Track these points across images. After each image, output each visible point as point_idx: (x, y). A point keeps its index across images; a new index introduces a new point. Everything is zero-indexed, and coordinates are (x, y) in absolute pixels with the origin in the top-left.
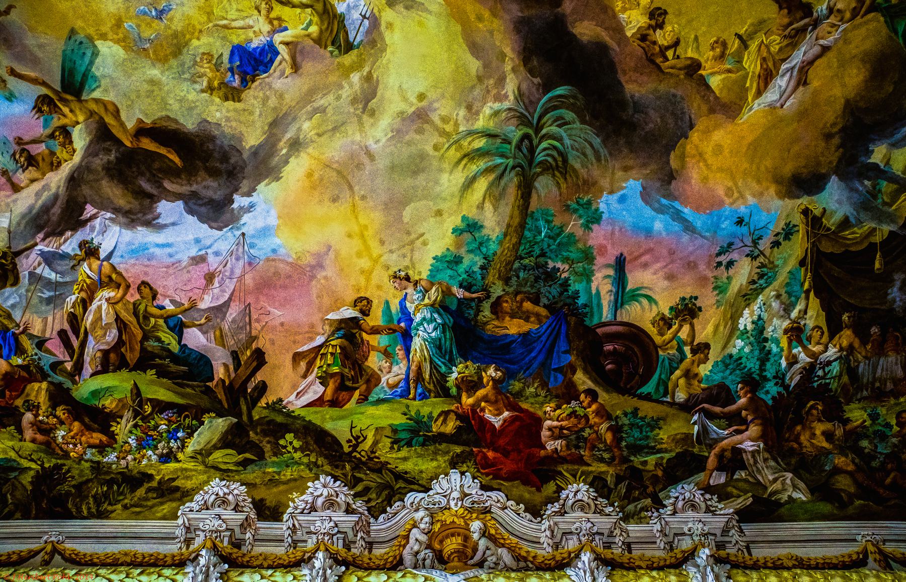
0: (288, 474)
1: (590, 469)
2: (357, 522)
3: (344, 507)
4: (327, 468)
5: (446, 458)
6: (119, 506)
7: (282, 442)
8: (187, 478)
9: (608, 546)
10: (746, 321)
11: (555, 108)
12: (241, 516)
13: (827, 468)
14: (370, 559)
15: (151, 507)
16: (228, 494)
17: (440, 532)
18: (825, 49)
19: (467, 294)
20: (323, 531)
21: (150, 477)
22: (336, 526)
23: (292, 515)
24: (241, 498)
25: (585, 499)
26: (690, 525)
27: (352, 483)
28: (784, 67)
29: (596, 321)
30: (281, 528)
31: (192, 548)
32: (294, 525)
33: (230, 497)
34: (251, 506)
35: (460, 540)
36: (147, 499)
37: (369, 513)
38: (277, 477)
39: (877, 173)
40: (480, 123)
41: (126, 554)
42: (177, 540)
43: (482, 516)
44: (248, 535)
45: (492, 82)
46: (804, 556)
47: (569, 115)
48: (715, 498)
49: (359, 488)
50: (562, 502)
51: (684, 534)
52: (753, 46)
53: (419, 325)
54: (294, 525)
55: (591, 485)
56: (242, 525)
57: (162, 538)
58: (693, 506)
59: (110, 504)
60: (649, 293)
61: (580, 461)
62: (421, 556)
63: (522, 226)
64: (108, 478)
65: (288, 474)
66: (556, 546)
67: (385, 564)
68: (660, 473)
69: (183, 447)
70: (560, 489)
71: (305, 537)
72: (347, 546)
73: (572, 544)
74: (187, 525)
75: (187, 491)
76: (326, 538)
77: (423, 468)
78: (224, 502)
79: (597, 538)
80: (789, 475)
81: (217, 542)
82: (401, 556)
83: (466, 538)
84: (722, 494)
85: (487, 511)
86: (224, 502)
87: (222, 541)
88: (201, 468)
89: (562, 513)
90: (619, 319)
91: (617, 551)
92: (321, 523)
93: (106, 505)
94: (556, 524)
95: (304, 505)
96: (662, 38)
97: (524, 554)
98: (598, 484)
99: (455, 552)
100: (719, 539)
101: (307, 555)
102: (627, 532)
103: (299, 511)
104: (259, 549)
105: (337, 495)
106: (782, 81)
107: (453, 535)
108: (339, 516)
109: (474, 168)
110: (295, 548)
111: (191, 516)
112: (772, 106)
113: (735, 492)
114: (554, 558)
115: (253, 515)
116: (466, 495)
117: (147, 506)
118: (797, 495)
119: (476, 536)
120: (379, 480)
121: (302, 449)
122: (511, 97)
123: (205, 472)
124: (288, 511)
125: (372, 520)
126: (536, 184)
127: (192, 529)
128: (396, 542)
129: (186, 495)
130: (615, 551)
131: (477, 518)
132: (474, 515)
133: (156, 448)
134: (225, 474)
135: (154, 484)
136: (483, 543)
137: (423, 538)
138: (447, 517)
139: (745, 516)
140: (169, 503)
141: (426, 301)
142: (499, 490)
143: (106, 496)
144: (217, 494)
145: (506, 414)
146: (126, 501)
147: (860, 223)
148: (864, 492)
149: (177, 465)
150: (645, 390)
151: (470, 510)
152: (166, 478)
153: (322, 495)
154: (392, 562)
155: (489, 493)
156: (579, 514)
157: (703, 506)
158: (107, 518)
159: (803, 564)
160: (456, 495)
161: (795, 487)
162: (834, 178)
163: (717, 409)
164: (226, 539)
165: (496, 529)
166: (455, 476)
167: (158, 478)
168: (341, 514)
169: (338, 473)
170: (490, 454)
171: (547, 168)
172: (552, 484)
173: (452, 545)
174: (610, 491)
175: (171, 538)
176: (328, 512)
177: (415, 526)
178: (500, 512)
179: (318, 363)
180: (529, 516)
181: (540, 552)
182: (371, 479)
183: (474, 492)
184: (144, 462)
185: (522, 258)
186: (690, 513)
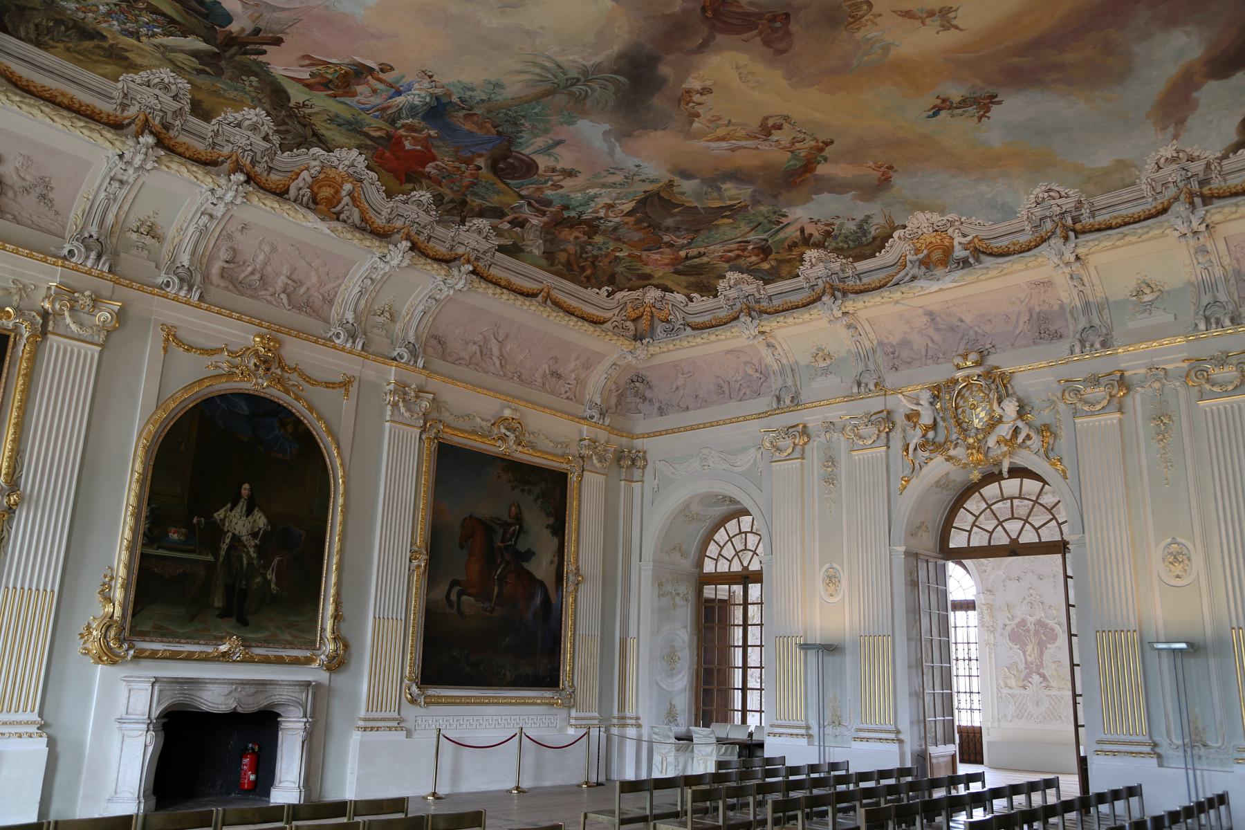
0: (233, 94)
1: (440, 188)
2: (268, 149)
3: (263, 134)
4: (267, 106)
5: (358, 142)
6: (61, 45)
7: (244, 78)
8: (140, 55)
9: (418, 233)
10: (592, 192)
11: (608, 81)
12: (178, 106)
13: (561, 247)
14: (267, 180)
15: (95, 62)
16: (173, 84)
17: (322, 180)
18: (757, 148)
19: (459, 103)
20: (239, 144)
21: (104, 38)
22: (251, 145)
23: (219, 123)
24: (182, 92)
25: (424, 202)
26: (470, 241)
27: (278, 122)
28: (734, 142)
29: (518, 150)
30: (208, 129)
31: (126, 114)
32: (218, 130)
33: (173, 87)
34: (189, 101)
35: (332, 191)
36: (93, 53)
37: (280, 147)
38: (222, 92)
39: (719, 189)
40: (561, 59)
41: (63, 94)
42: (114, 101)
43: (355, 182)
44: (178, 122)
45: (590, 51)
46: (513, 282)
47: (611, 87)
48: (494, 233)
49: (282, 128)
50: (409, 196)
51: (463, 244)
52: (731, 128)
53: (412, 94)
54: (218, 130)
55: (434, 196)
56: (174, 112)
57: (100, 93)
58: (480, 232)
59: (52, 39)
60: (559, 157)
61: (440, 184)
62: (302, 192)
63: (527, 102)
64: (58, 17)
65: (233, 94)
66: (389, 221)
67: (276, 189)
68: (477, 209)
69: (154, 35)
70: (414, 189)
71: (224, 143)
72: (254, 162)
73: (399, 223)
74: (125, 91)
75: (136, 65)
76: (240, 151)
77: (337, 138)
78: (166, 88)
79: (416, 225)
80: (541, 241)
81: (150, 119)
82: (289, 186)
83: (337, 192)
84: (499, 234)
85: (361, 181)
86: (166, 88)
87: (154, 119)
88: (159, 55)
89: (405, 202)
90: (531, 156)
91: (422, 238)
92: (241, 138)
93: (47, 38)
94: (397, 207)
95: (233, 120)
96: (696, 98)
97: (368, 218)
98: (438, 200)
99: (326, 198)
100: (480, 255)
101: (220, 159)
102: (434, 230)
103: (226, 122)
104: (183, 138)
105: (263, 125)
106: (724, 144)
107: (330, 186)
108: (257, 140)
109: (532, 69)
110: (213, 149)
111: (132, 85)
112: (708, 147)
113: (507, 235)
114: (383, 228)
115: (187, 108)
116: (353, 166)
117: (90, 58)
118: (534, 251)
119: (344, 193)
120: (300, 130)
121: (256, 88)
122: (591, 63)
123: (160, 59)
124: (218, 118)
125: (279, 152)
126: (557, 95)
127: (129, 97)
128: (289, 175)
129: (134, 67)
130: (420, 238)
131: (351, 182)
132: (351, 180)
133: (125, 24)
134: (178, 69)
135: (105, 45)
136: (346, 199)
137: (309, 180)
138: (332, 173)
139: (502, 249)
140: (113, 66)
141: (430, 90)
142: (377, 173)
143: (49, 30)
144: (162, 80)
145: (419, 148)
146: (70, 45)
147: (689, 196)
148: (569, 265)
149: (136, 43)
150: (509, 181)
151: (350, 175)
152: (119, 46)
153: (251, 119)
154: (281, 188)
155: (368, 172)
156: (415, 208)
157: (485, 234)
158: (46, 49)
159: (510, 288)
160: (347, 163)
161: (538, 247)
162: (699, 181)
163: (537, 205)
164: (158, 119)
165: (359, 194)
166: (355, 152)
167: (111, 42)
168: (259, 138)
169: (273, 112)
170: (388, 154)
171: (572, 95)
172: (412, 185)
173: (326, 192)
174: (442, 204)
175: (109, 97)
176: (249, 133)
177: (307, 169)
178: (368, 185)
179: (320, 67)
180: (384, 195)
181: (378, 221)
182: (294, 126)
183: (360, 167)
184: (104, 25)
185: (510, 110)
186: (475, 235)
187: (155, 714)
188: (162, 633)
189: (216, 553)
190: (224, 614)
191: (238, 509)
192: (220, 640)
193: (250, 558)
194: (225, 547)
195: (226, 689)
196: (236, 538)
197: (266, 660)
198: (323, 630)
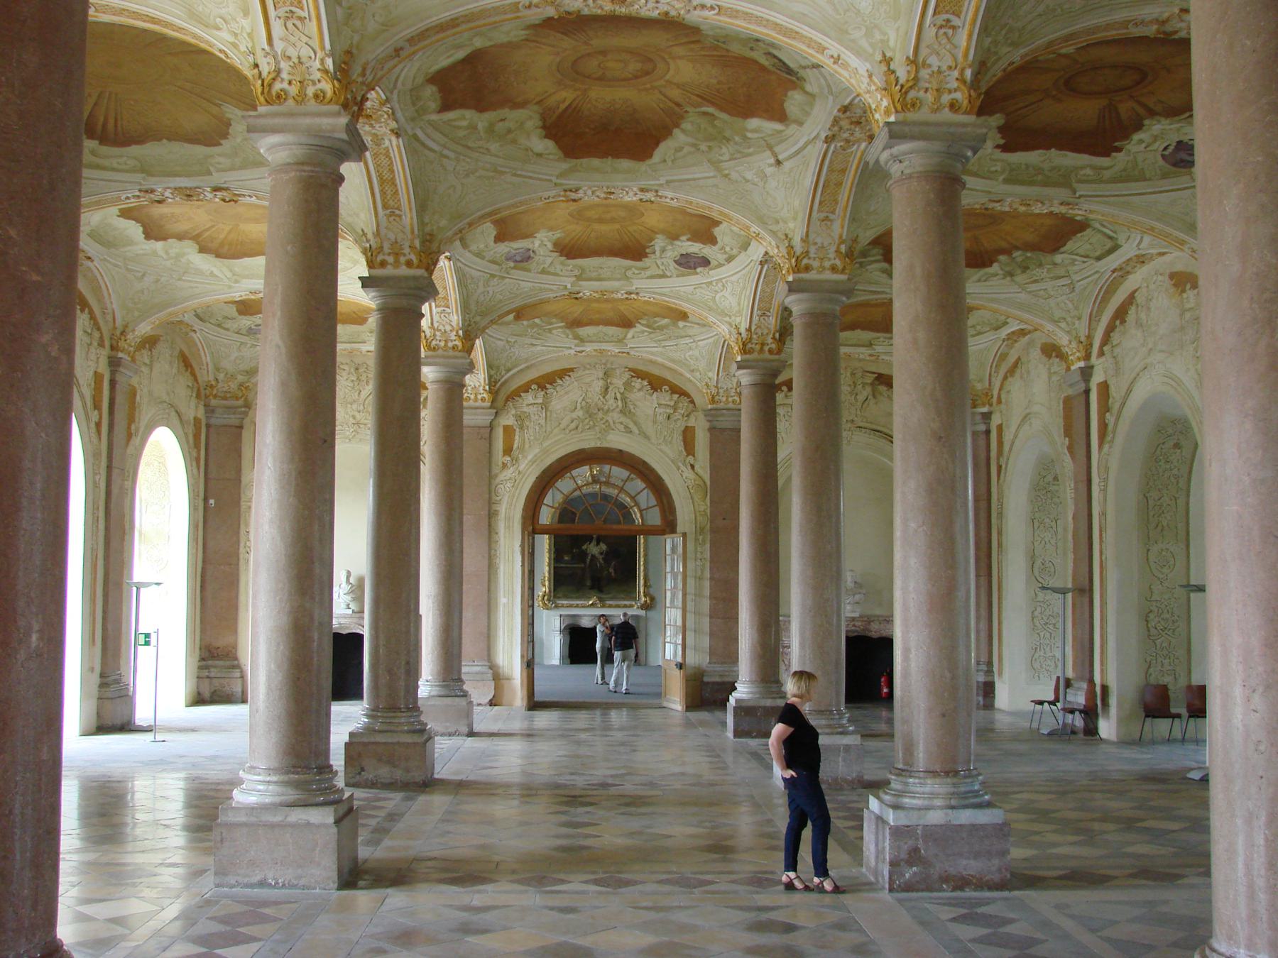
187: (562, 628)
188: (566, 597)
189: (585, 562)
190: (592, 588)
191: (592, 544)
192: (590, 598)
193: (601, 564)
194: (588, 560)
195: (590, 618)
196: (593, 556)
197: (610, 606)
198: (639, 592)
